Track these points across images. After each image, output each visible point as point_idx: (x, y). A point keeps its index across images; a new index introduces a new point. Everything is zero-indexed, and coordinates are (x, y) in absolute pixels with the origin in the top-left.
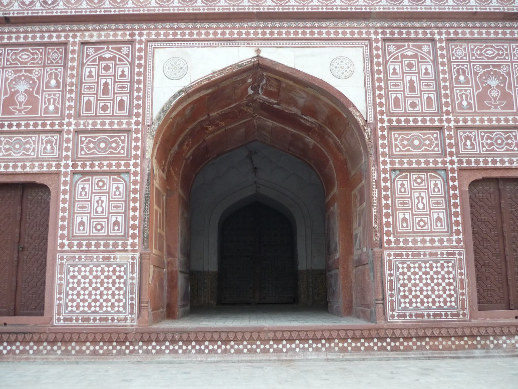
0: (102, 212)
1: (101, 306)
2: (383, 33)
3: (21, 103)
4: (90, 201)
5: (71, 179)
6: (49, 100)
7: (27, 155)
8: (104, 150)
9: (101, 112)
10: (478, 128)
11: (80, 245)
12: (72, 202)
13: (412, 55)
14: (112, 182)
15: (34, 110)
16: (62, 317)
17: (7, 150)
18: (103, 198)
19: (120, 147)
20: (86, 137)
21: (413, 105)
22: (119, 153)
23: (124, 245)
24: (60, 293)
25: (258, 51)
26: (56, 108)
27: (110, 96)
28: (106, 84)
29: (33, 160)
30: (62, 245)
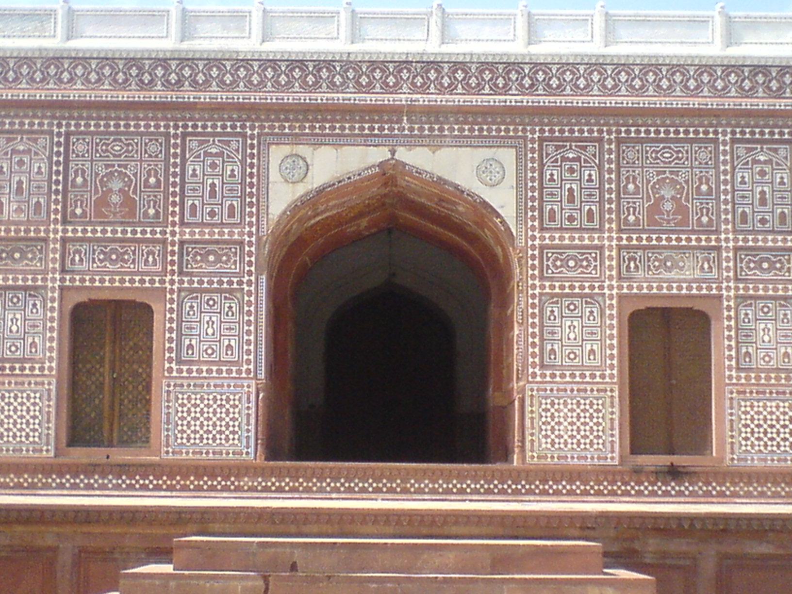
3: (115, 205)
5: (178, 296)
13: (574, 158)
25: (393, 153)
28: (213, 185)
30: (170, 370)
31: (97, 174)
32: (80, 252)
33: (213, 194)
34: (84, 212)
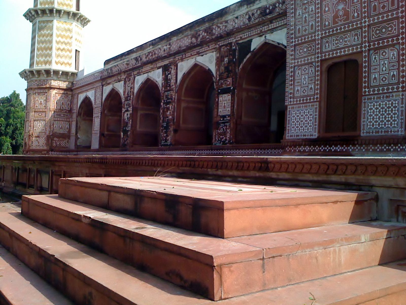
0: (386, 70)
1: (385, 124)
3: (341, 16)
4: (379, 65)
6: (354, 10)
7: (346, 45)
9: (382, 10)
12: (369, 66)
14: (390, 52)
15: (348, 19)
16: (365, 131)
17: (336, 44)
18: (386, 62)
19: (394, 29)
20: (375, 28)
22: (393, 33)
23: (398, 88)
26: (358, 14)
30: (365, 92)
32: (327, 42)
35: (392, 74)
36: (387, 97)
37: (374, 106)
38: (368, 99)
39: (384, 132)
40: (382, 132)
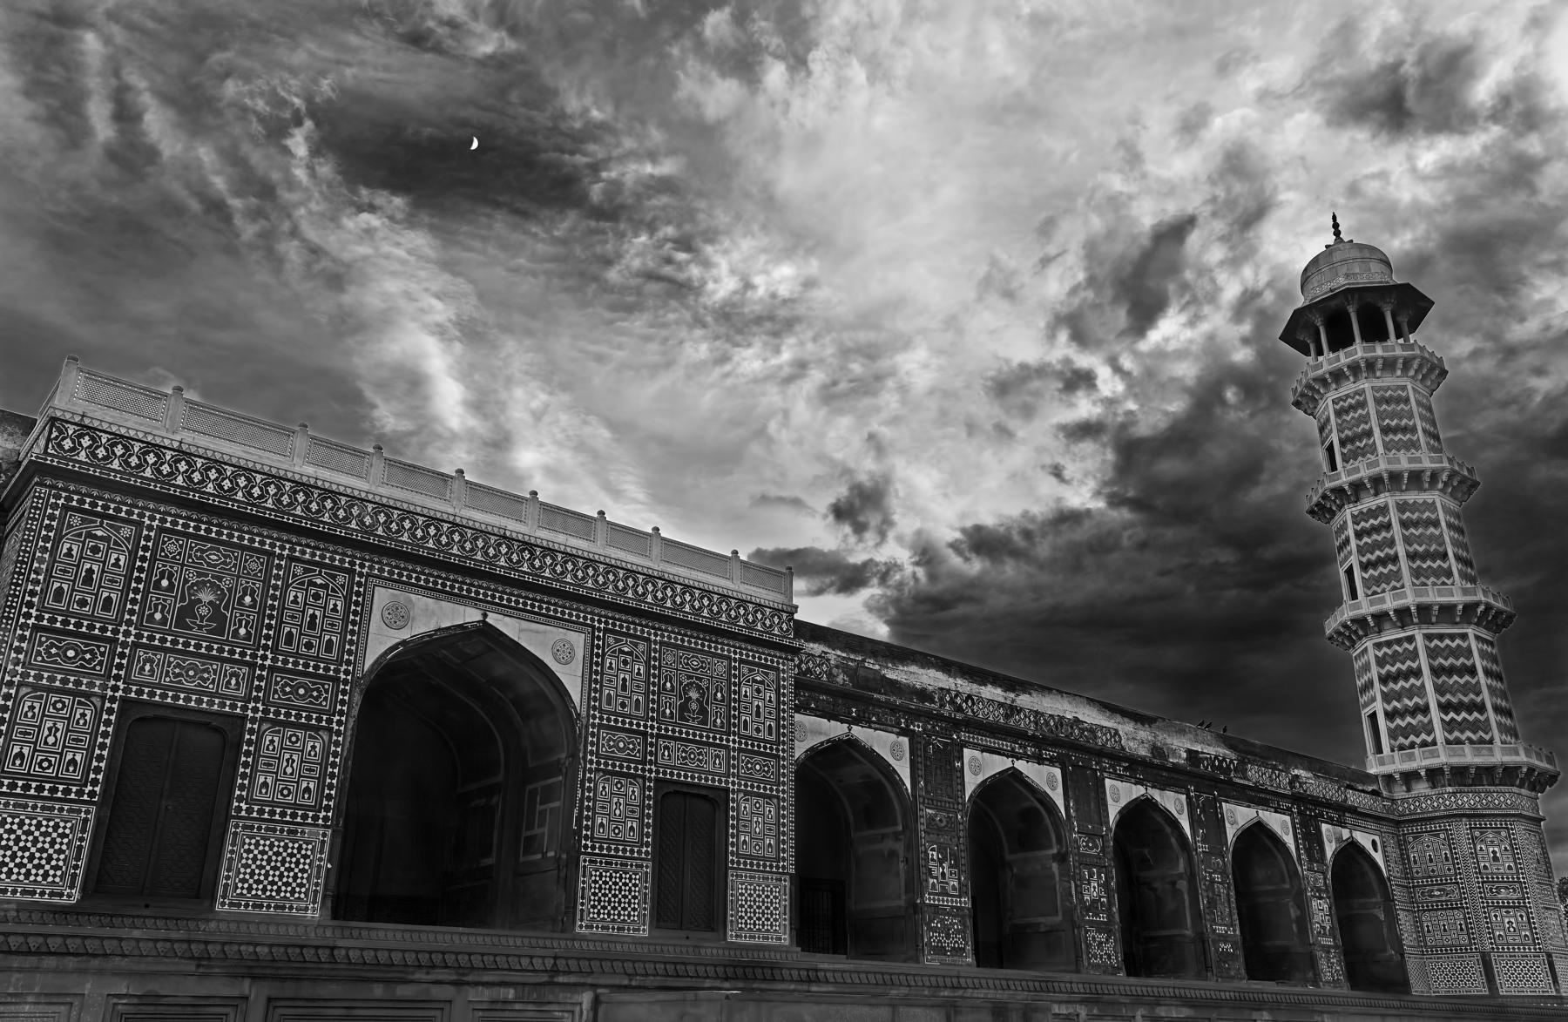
1: (279, 891)
2: (606, 623)
3: (202, 617)
8: (303, 697)
10: (676, 739)
11: (261, 812)
17: (177, 675)
21: (623, 705)
23: (315, 818)
24: (229, 870)
25: (485, 616)
26: (248, 633)
27: (317, 632)
28: (313, 616)
29: (211, 695)
30: (239, 809)
31: (186, 581)
32: (151, 661)
33: (312, 625)
34: (164, 619)
35: (304, 785)
36: (245, 827)
37: (257, 845)
38: (245, 827)
39: (276, 907)
40: (269, 907)
